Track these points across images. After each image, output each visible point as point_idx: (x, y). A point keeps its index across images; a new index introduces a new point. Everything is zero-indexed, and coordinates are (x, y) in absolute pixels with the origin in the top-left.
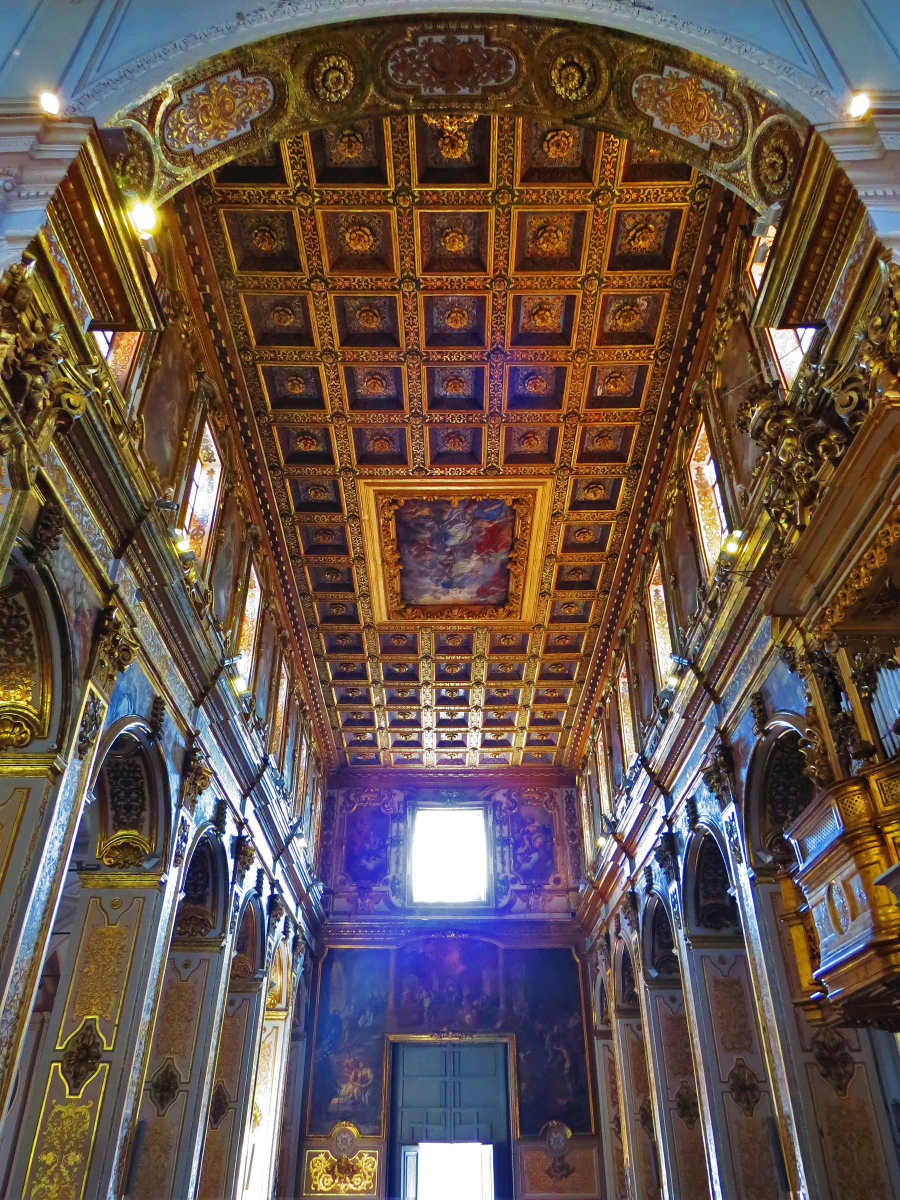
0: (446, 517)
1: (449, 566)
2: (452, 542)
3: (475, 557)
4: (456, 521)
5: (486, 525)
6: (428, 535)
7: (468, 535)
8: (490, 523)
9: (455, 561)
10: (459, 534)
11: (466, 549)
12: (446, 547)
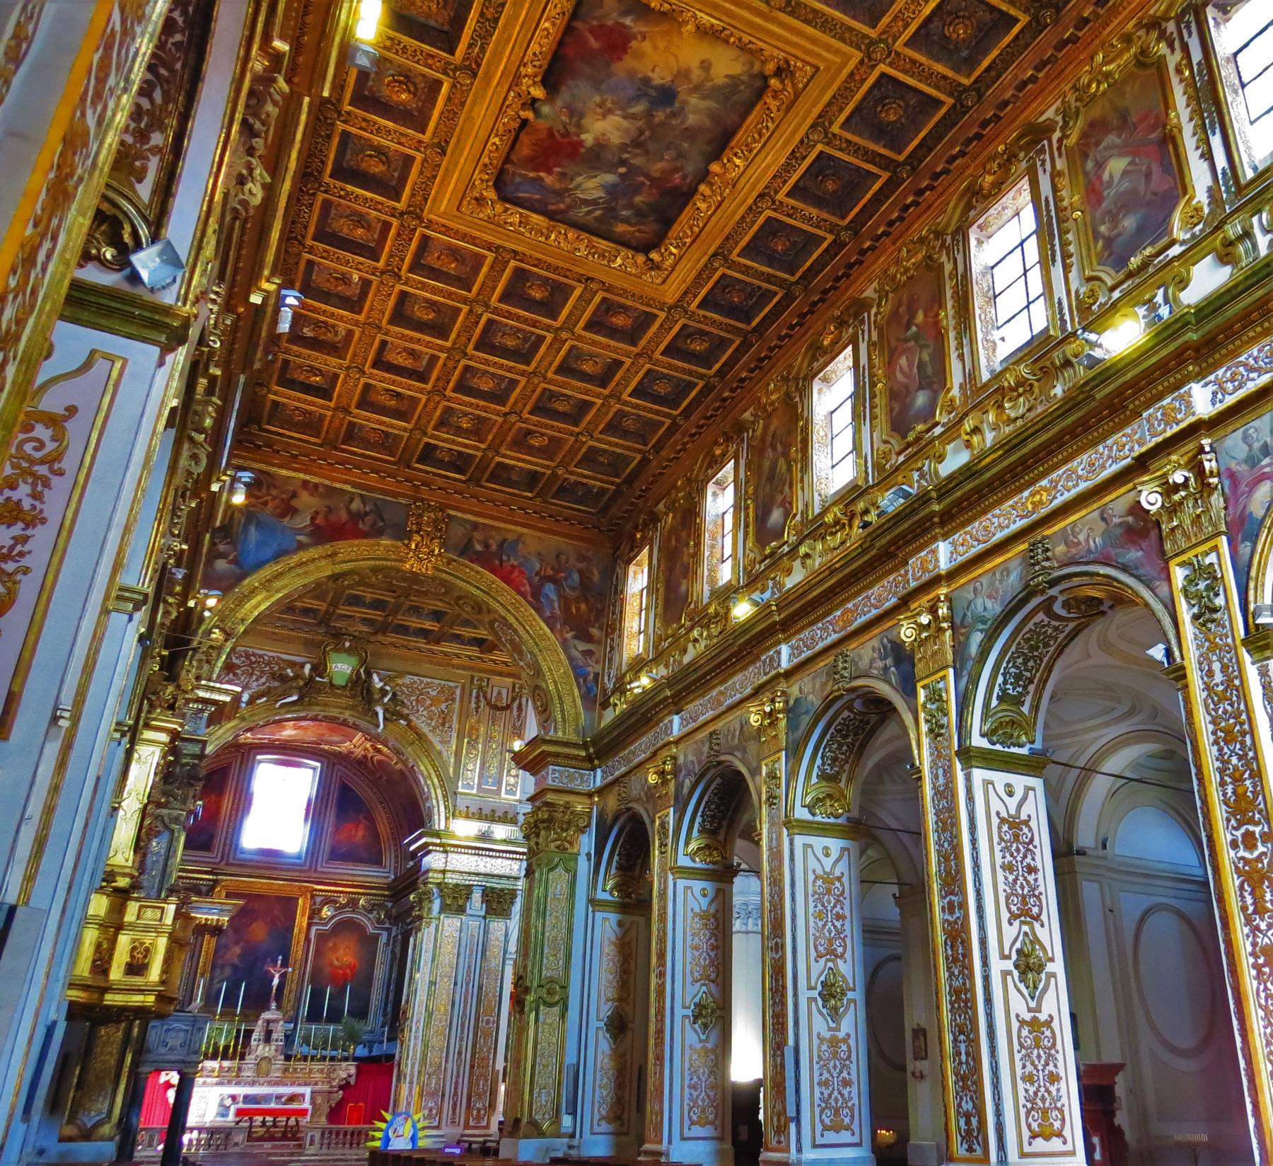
0: (598, 213)
1: (636, 143)
2: (610, 178)
3: (588, 139)
4: (586, 202)
5: (549, 180)
6: (638, 199)
7: (579, 179)
8: (542, 179)
9: (623, 147)
10: (592, 186)
11: (596, 158)
12: (621, 175)
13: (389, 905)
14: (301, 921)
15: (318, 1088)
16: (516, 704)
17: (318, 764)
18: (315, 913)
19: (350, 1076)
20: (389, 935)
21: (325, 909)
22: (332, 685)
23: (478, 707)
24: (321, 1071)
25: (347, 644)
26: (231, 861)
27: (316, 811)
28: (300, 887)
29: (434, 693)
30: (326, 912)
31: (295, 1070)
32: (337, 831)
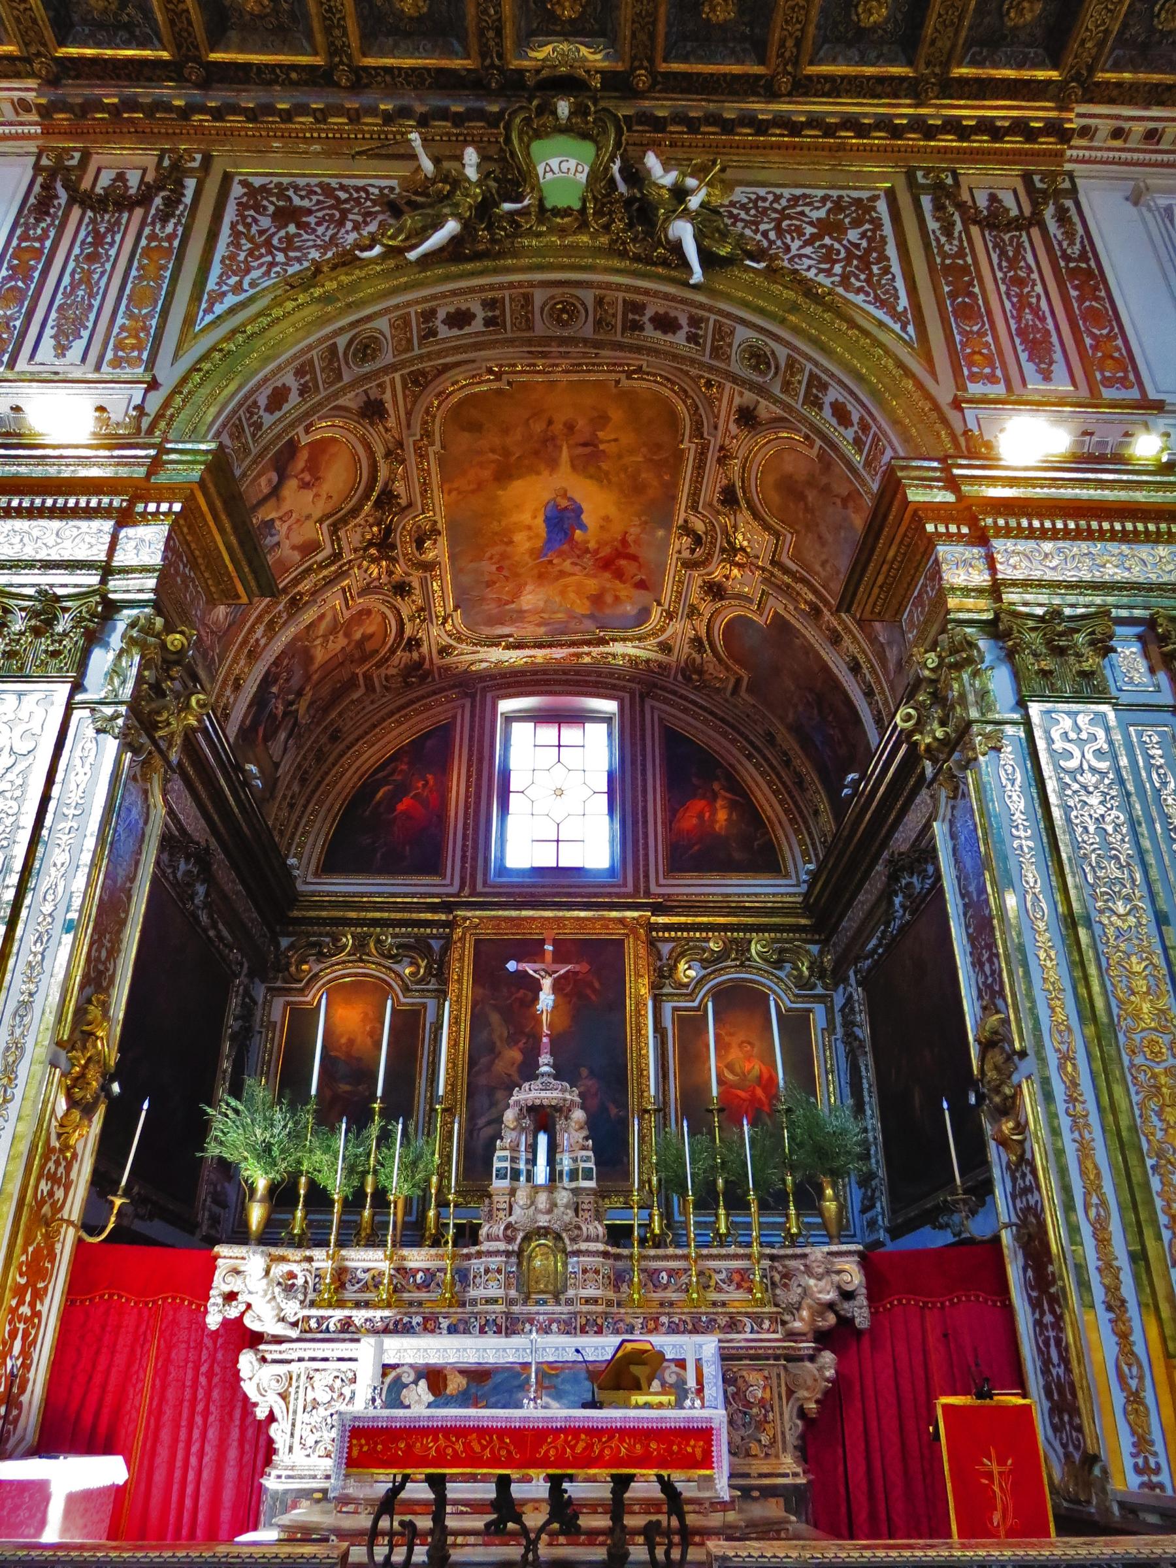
13: (814, 949)
14: (639, 987)
15: (740, 1339)
16: (1049, 213)
17: (609, 706)
18: (662, 975)
19: (848, 1296)
20: (830, 1011)
21: (682, 966)
22: (543, 212)
23: (948, 230)
24: (742, 1279)
25: (563, 108)
26: (480, 888)
27: (623, 792)
28: (621, 921)
29: (822, 213)
30: (687, 972)
31: (652, 1276)
32: (672, 812)
